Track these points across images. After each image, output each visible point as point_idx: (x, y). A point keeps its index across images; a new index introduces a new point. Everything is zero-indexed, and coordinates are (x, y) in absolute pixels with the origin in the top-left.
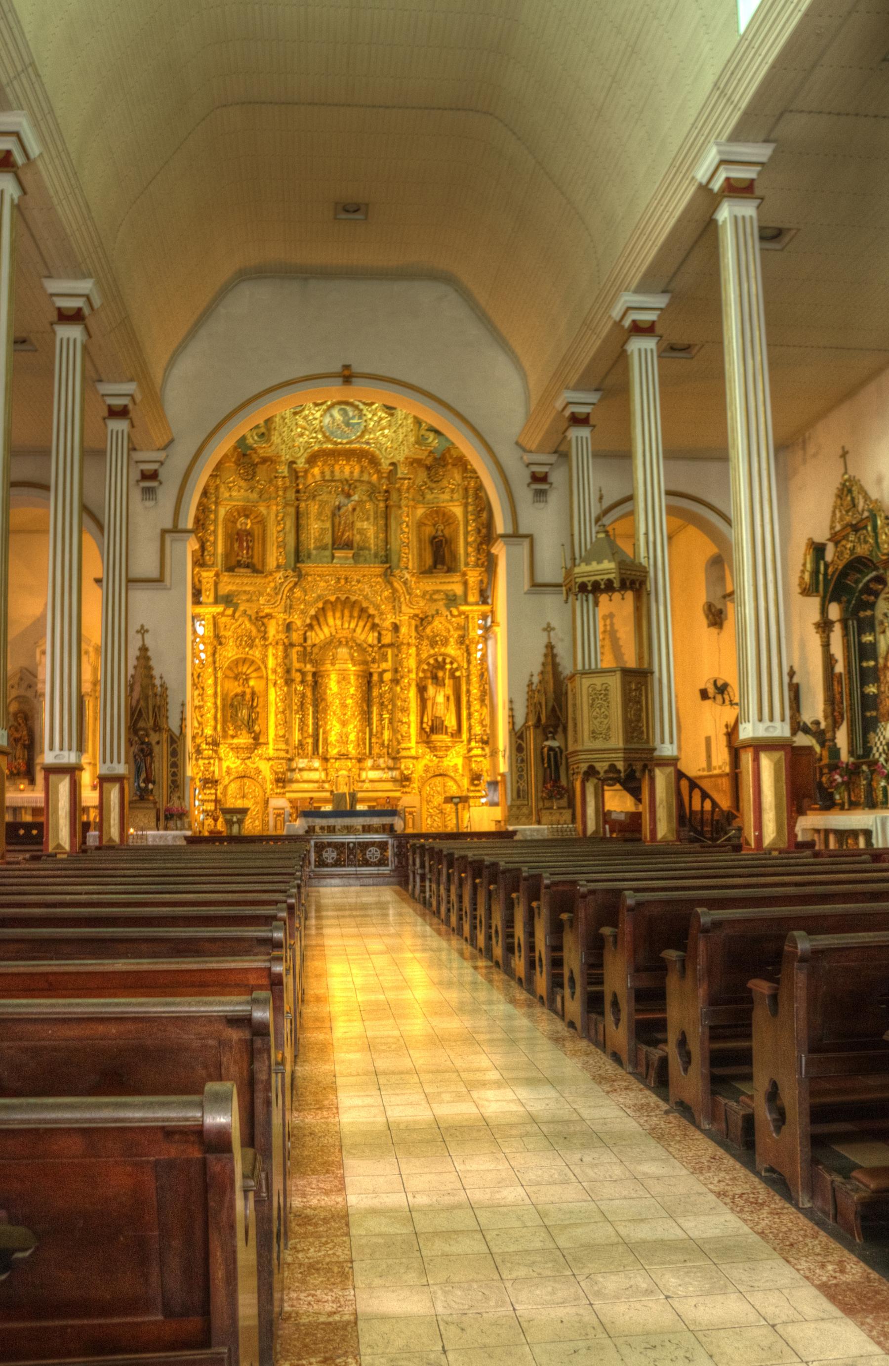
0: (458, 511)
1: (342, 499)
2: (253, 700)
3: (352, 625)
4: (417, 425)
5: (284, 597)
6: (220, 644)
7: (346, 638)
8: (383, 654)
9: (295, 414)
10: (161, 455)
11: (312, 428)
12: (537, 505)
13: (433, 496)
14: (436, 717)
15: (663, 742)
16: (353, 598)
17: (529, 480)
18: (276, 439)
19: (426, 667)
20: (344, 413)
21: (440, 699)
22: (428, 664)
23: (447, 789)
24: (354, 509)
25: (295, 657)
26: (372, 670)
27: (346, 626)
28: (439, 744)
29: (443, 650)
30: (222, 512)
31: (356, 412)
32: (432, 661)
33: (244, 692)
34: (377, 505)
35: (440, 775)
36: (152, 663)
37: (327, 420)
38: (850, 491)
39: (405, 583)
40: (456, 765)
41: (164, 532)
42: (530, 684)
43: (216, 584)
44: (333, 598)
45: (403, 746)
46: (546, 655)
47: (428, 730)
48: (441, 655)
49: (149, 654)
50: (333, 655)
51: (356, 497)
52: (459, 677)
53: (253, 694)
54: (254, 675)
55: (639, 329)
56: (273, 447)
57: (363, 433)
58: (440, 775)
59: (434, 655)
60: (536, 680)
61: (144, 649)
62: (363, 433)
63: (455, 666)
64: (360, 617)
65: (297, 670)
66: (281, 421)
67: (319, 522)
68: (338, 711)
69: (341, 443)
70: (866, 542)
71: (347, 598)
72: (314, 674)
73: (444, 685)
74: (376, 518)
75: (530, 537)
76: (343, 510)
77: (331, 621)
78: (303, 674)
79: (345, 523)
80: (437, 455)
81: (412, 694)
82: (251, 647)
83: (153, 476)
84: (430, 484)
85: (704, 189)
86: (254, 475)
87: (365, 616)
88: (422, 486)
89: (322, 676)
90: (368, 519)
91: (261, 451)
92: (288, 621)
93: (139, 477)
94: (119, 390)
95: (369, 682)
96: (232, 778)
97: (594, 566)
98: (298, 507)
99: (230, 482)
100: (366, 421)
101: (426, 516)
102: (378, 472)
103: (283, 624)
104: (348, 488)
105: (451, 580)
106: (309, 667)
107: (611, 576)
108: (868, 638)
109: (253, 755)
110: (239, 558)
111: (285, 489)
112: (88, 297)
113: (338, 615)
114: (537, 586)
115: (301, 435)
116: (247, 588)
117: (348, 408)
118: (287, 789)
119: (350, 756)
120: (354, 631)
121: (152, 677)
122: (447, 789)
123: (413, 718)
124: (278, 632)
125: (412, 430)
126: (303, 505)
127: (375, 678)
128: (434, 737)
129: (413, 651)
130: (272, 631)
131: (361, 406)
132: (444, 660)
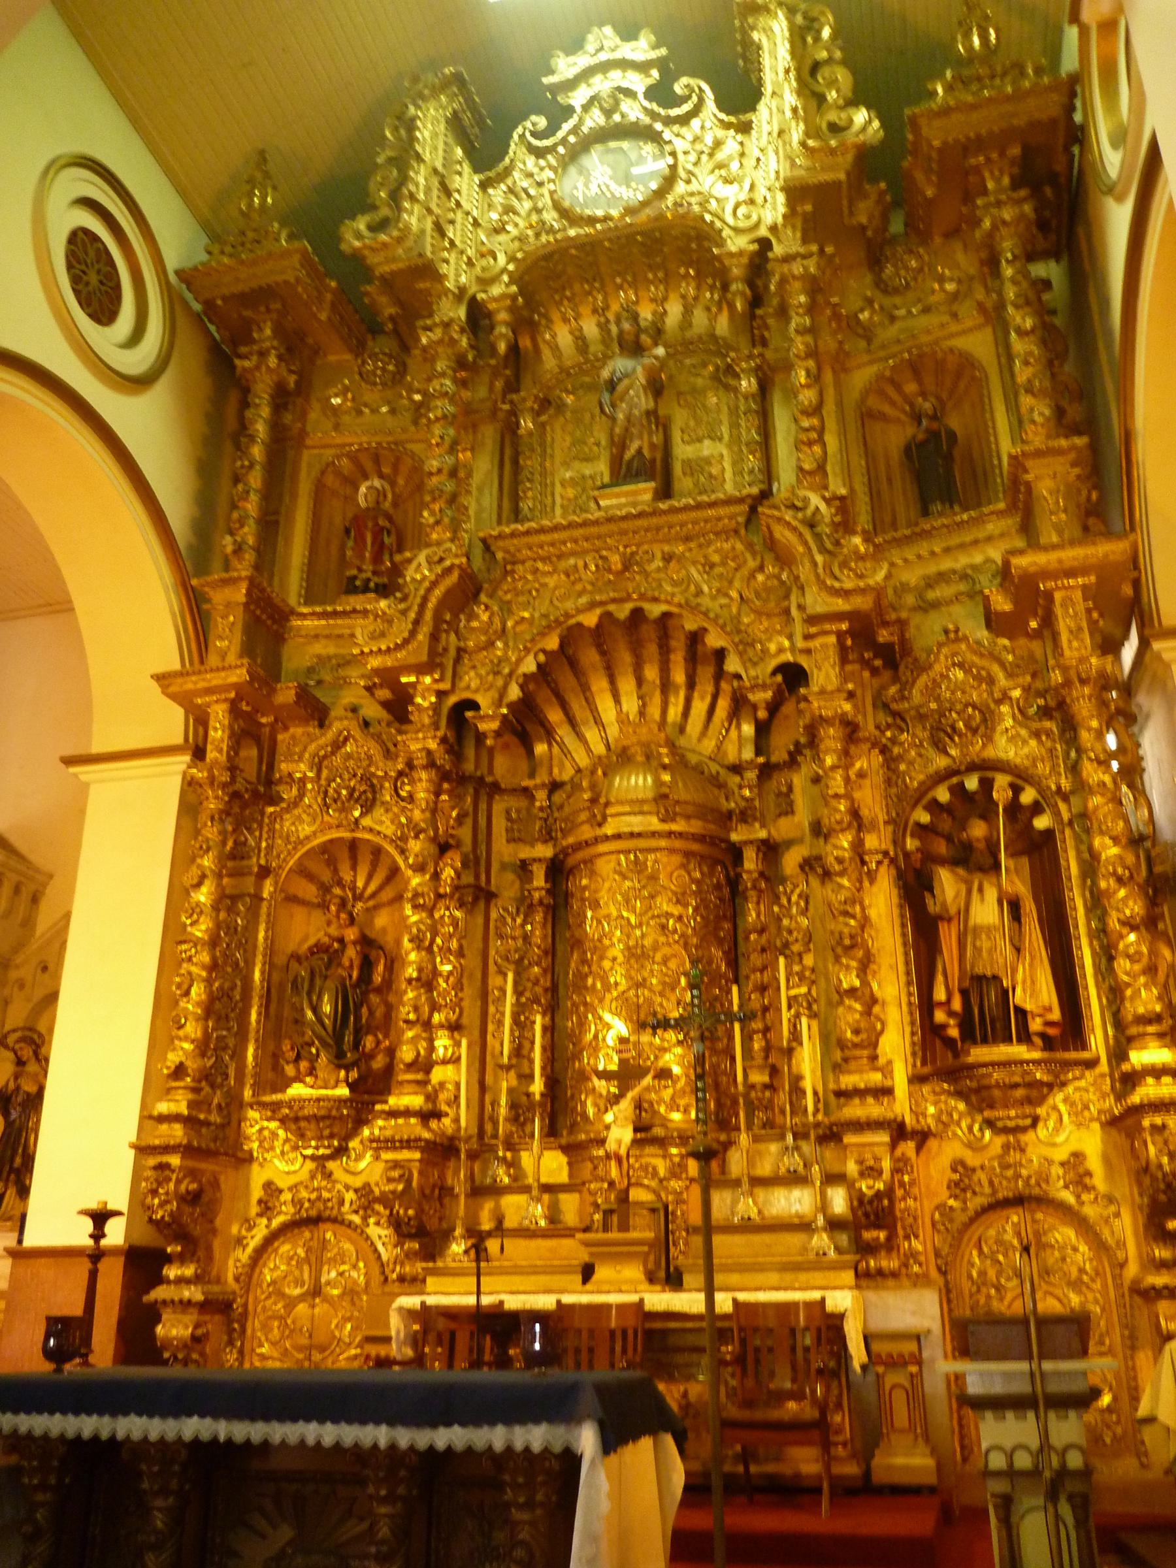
0: (978, 344)
2: (367, 965)
3: (674, 712)
4: (813, 104)
5: (428, 615)
6: (274, 800)
7: (646, 745)
8: (779, 794)
11: (527, 205)
13: (898, 325)
14: (979, 979)
16: (655, 610)
18: (413, 218)
19: (925, 818)
21: (986, 911)
22: (934, 806)
23: (1052, 1257)
25: (499, 825)
26: (734, 837)
27: (654, 712)
28: (997, 1076)
29: (976, 748)
31: (649, 148)
32: (943, 795)
33: (341, 940)
34: (736, 390)
35: (1019, 1201)
40: (1078, 1156)
44: (590, 620)
45: (848, 1081)
47: (954, 1032)
48: (972, 768)
50: (593, 786)
52: (1049, 834)
53: (367, 942)
54: (387, 894)
56: (409, 243)
58: (1019, 1201)
62: (670, 180)
63: (1028, 796)
64: (691, 685)
65: (504, 867)
66: (435, 183)
67: (577, 465)
68: (618, 976)
69: (607, 218)
71: (637, 615)
72: (558, 870)
73: (997, 866)
74: (734, 425)
76: (620, 388)
79: (628, 419)
81: (882, 901)
82: (367, 809)
84: (880, 300)
86: (402, 370)
87: (705, 674)
88: (862, 310)
89: (571, 871)
91: (373, 259)
92: (452, 700)
95: (734, 883)
96: (276, 1222)
98: (510, 428)
99: (336, 395)
100: (673, 154)
101: (878, 387)
103: (436, 708)
105: (981, 535)
109: (351, 1145)
110: (354, 572)
113: (627, 685)
115: (499, 230)
117: (625, 145)
118: (440, 1264)
119: (658, 1131)
120: (682, 730)
122: (1052, 1257)
123: (892, 986)
125: (795, 110)
126: (527, 424)
127: (751, 862)
128: (979, 1054)
131: (658, 126)
132: (987, 785)
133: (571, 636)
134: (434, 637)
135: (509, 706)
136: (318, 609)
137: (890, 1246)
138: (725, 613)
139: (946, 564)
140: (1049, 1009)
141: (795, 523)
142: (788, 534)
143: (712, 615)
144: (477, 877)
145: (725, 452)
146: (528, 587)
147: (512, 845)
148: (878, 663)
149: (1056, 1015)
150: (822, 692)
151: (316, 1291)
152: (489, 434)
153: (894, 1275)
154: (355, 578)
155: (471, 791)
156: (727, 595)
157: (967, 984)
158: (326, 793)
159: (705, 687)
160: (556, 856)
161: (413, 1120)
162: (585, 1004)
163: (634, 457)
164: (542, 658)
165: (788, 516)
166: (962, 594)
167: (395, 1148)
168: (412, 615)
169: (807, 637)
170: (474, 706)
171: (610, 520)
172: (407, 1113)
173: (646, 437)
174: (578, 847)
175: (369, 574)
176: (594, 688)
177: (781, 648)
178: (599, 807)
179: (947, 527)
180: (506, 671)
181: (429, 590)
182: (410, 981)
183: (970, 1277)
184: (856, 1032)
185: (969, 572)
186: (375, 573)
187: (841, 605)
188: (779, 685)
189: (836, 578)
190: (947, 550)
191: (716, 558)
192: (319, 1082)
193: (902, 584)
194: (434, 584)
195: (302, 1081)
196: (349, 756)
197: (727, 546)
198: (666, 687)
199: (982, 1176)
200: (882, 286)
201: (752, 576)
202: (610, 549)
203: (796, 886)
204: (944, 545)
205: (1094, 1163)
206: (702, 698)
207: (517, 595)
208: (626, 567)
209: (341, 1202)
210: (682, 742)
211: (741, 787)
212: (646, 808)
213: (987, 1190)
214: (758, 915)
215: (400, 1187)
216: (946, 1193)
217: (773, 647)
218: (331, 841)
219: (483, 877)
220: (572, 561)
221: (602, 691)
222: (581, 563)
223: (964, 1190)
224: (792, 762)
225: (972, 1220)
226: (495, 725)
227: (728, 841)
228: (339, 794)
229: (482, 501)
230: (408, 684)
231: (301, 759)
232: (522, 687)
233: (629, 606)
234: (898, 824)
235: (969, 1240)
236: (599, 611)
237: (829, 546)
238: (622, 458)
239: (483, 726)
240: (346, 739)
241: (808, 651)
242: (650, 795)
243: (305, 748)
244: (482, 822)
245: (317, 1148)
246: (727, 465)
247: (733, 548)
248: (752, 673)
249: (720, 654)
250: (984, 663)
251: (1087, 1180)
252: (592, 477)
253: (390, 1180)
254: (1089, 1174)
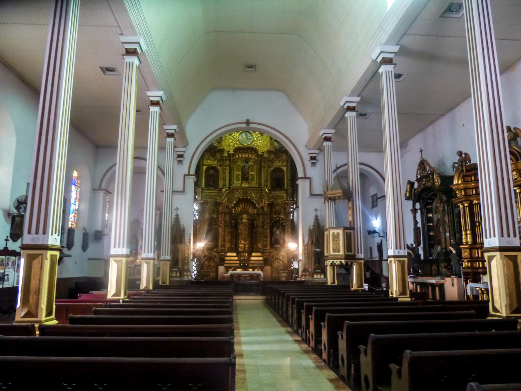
0: (285, 169)
1: (244, 164)
9: (230, 135)
10: (183, 149)
12: (313, 168)
15: (358, 253)
17: (309, 159)
18: (223, 143)
20: (246, 135)
24: (249, 167)
30: (205, 168)
36: (180, 220)
37: (240, 137)
38: (423, 164)
41: (185, 175)
42: (310, 230)
43: (202, 192)
46: (315, 219)
49: (179, 217)
51: (250, 164)
55: (350, 109)
57: (253, 142)
59: (275, 218)
60: (312, 228)
61: (177, 215)
62: (253, 142)
70: (430, 182)
75: (310, 178)
77: (241, 205)
78: (231, 223)
80: (278, 149)
81: (268, 231)
83: (181, 156)
85: (375, 61)
86: (215, 155)
90: (254, 171)
93: (176, 156)
94: (171, 128)
97: (334, 192)
102: (258, 155)
104: (247, 161)
106: (233, 222)
107: (340, 195)
108: (430, 215)
111: (226, 160)
112: (161, 97)
113: (243, 203)
114: (312, 195)
115: (232, 142)
116: (212, 194)
121: (180, 225)
123: (268, 239)
124: (223, 209)
129: (269, 216)
130: (221, 209)
151: (210, 265)
152: (228, 168)
177: (261, 205)
178: (242, 219)
200: (275, 156)
224: (260, 214)
234: (271, 222)
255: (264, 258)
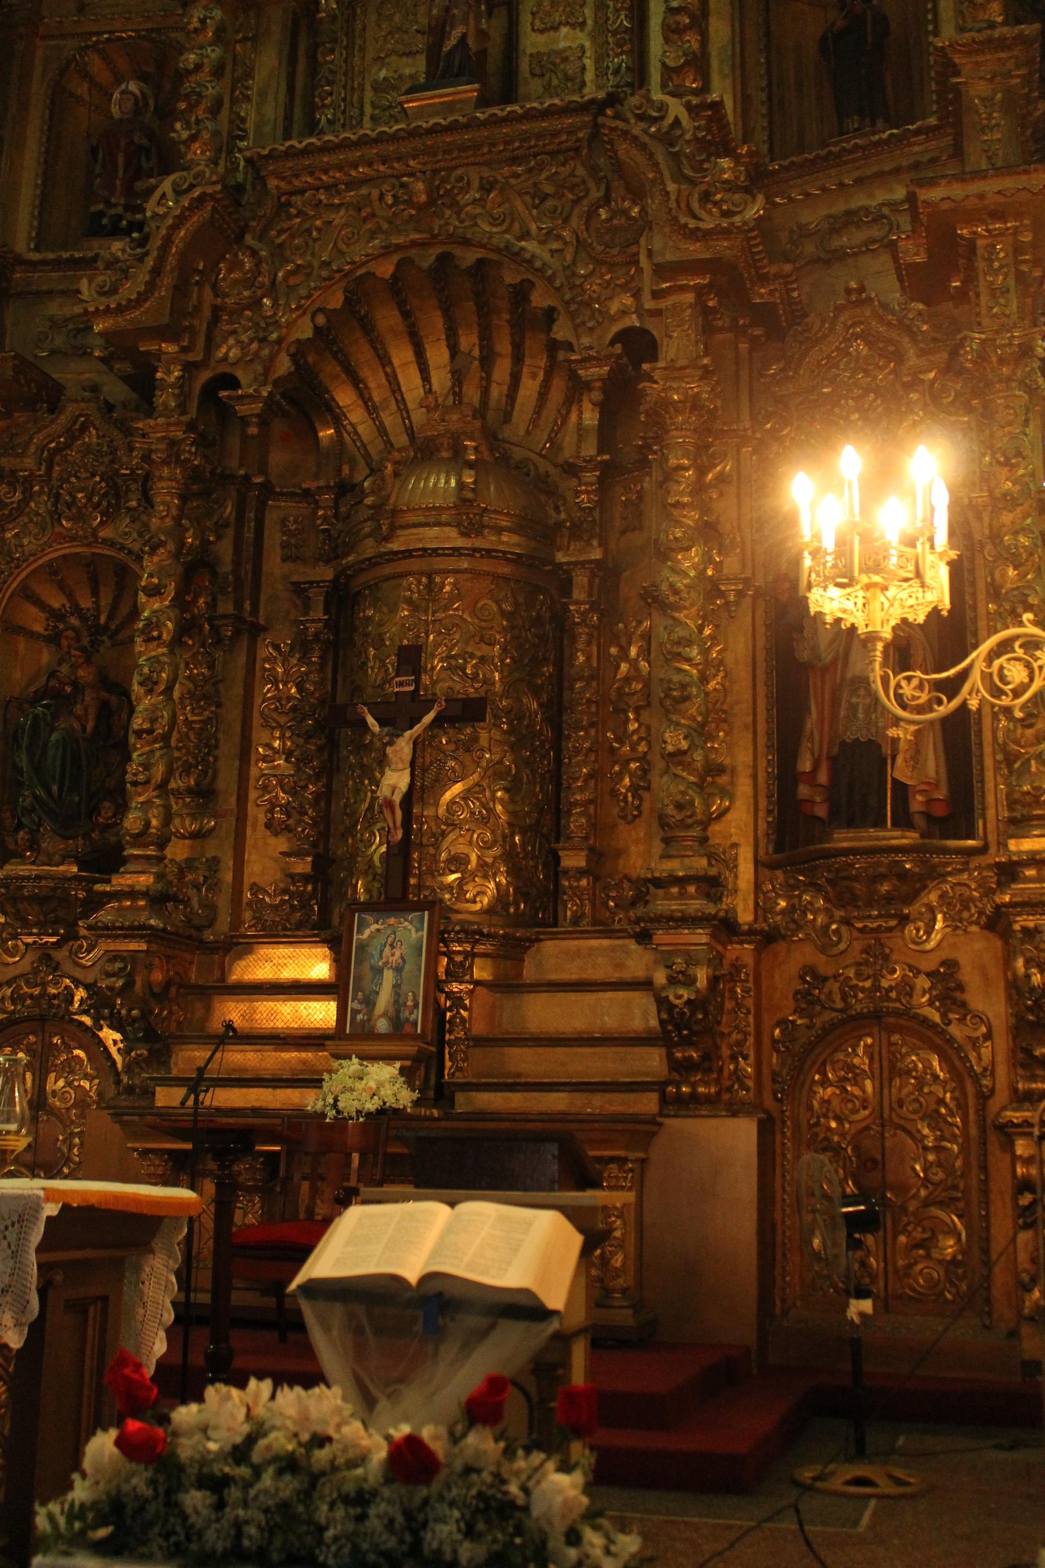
5: (172, 261)
16: (468, 257)
25: (274, 540)
26: (561, 558)
33: (75, 684)
39: (667, 139)
44: (386, 269)
47: (821, 811)
64: (518, 359)
103: (182, 384)
110: (101, 206)
113: (438, 355)
120: (507, 417)
128: (843, 839)
133: (359, 293)
134: (180, 290)
135: (276, 383)
136: (51, 256)
137: (708, 1063)
138: (555, 263)
139: (859, 201)
140: (937, 786)
141: (646, 139)
142: (634, 152)
143: (538, 264)
144: (238, 604)
145: (587, 44)
146: (307, 225)
147: (289, 566)
148: (758, 332)
149: (941, 794)
150: (670, 367)
153: (710, 1101)
154: (101, 214)
155: (234, 494)
156: (559, 237)
157: (835, 751)
158: (58, 496)
159: (536, 362)
160: (337, 578)
161: (142, 903)
162: (362, 766)
163: (455, 47)
164: (321, 320)
165: (637, 129)
166: (875, 241)
167: (117, 937)
168: (150, 262)
169: (656, 295)
170: (232, 382)
171: (414, 134)
172: (132, 894)
173: (472, 22)
174: (361, 568)
175: (119, 210)
176: (396, 362)
177: (622, 309)
179: (863, 148)
180: (274, 336)
181: (174, 228)
182: (139, 733)
183: (810, 1108)
184: (679, 807)
185: (886, 211)
186: (127, 208)
187: (695, 250)
188: (619, 357)
189: (695, 217)
190: (859, 181)
191: (549, 189)
192: (42, 858)
193: (801, 227)
194: (180, 220)
195: (22, 856)
196: (88, 449)
197: (565, 170)
198: (487, 360)
199: (834, 986)
201: (591, 214)
202: (411, 175)
203: (640, 622)
204: (857, 174)
205: (968, 975)
206: (534, 376)
207: (292, 237)
208: (432, 202)
209: (71, 1002)
210: (507, 433)
211: (578, 493)
212: (444, 518)
213: (839, 1005)
214: (588, 658)
215: (120, 983)
216: (791, 1004)
217: (614, 307)
218: (65, 557)
219: (247, 605)
220: (364, 191)
221: (405, 365)
222: (375, 193)
223: (811, 1003)
225: (820, 1038)
226: (257, 407)
227: (552, 562)
228: (74, 498)
229: (262, 111)
230: (148, 353)
231: (23, 455)
232: (293, 356)
233: (437, 251)
235: (814, 1063)
236: (396, 258)
237: (688, 172)
238: (440, 51)
239: (242, 409)
240: (84, 428)
241: (658, 313)
242: (451, 500)
243: (31, 438)
244: (249, 535)
245: (38, 935)
246: (588, 62)
247: (572, 174)
248: (586, 341)
249: (550, 315)
250: (894, 335)
251: (958, 995)
252: (411, 77)
253: (109, 975)
254: (961, 988)
255: (662, 1003)
